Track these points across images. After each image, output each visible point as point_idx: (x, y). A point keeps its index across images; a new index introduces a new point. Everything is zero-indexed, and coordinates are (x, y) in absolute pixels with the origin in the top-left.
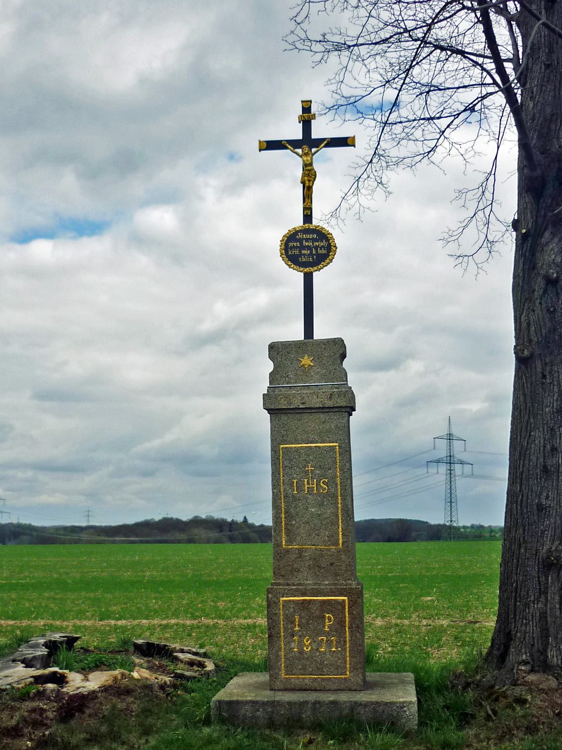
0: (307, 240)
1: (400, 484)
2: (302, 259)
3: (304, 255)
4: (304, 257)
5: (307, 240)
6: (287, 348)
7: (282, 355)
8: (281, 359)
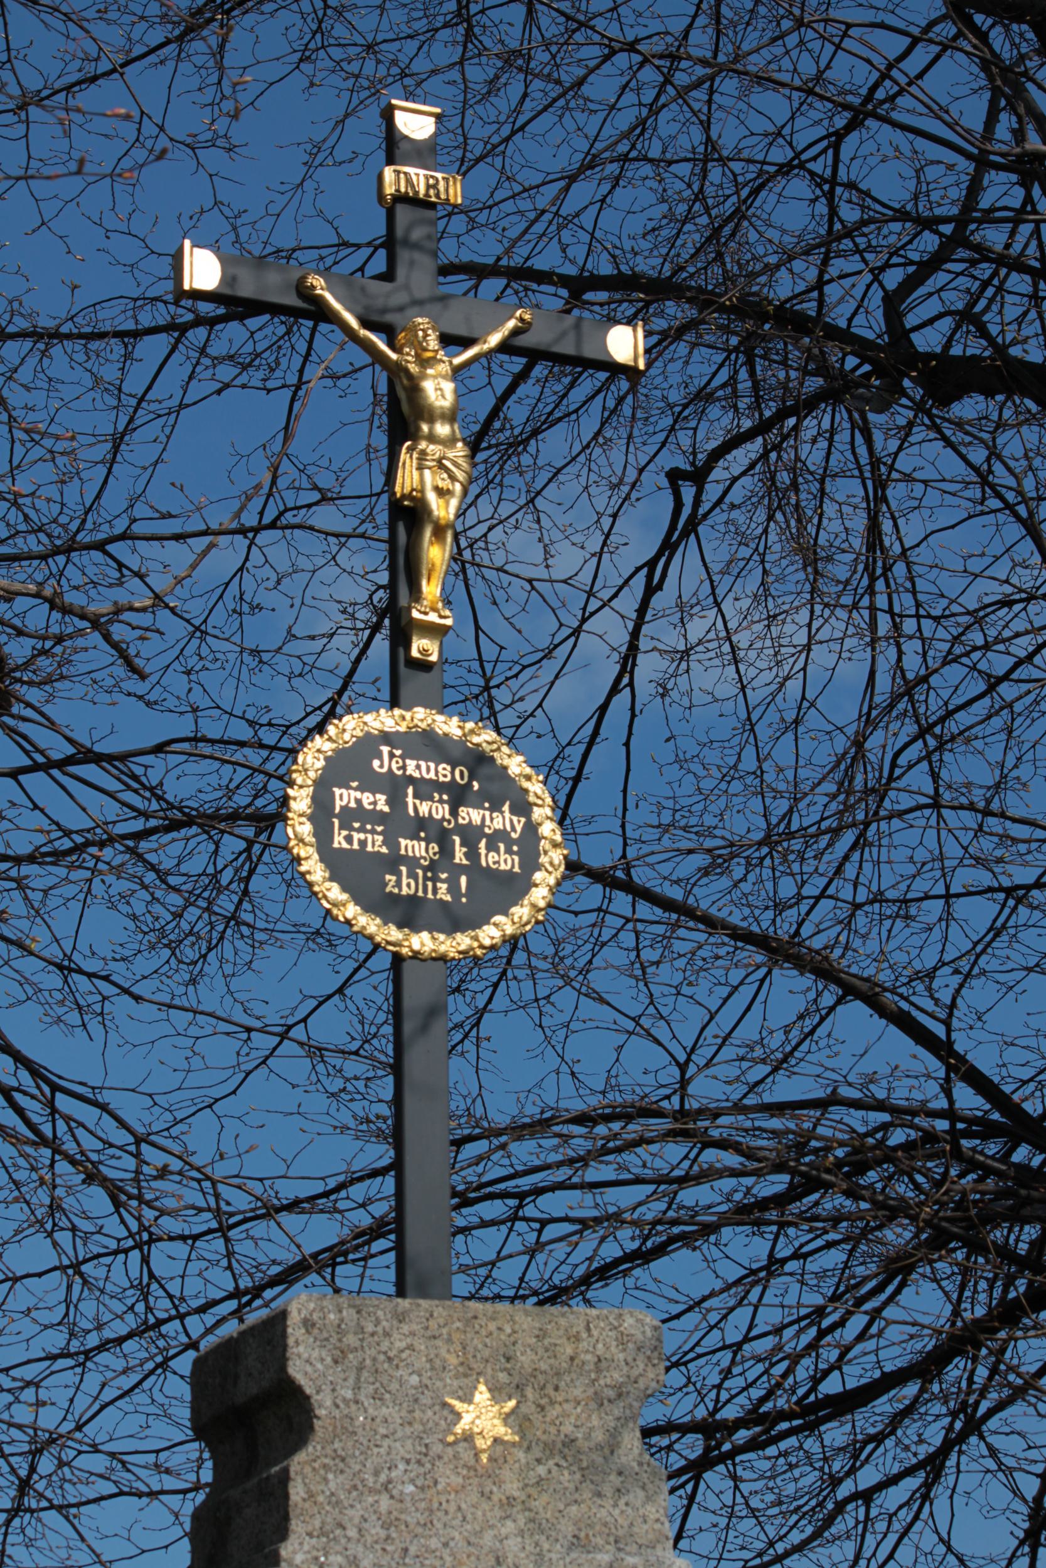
0: (425, 789)
1: (883, 1297)
2: (398, 884)
3: (412, 862)
4: (412, 875)
5: (425, 789)
6: (387, 1334)
7: (360, 1369)
8: (357, 1388)
